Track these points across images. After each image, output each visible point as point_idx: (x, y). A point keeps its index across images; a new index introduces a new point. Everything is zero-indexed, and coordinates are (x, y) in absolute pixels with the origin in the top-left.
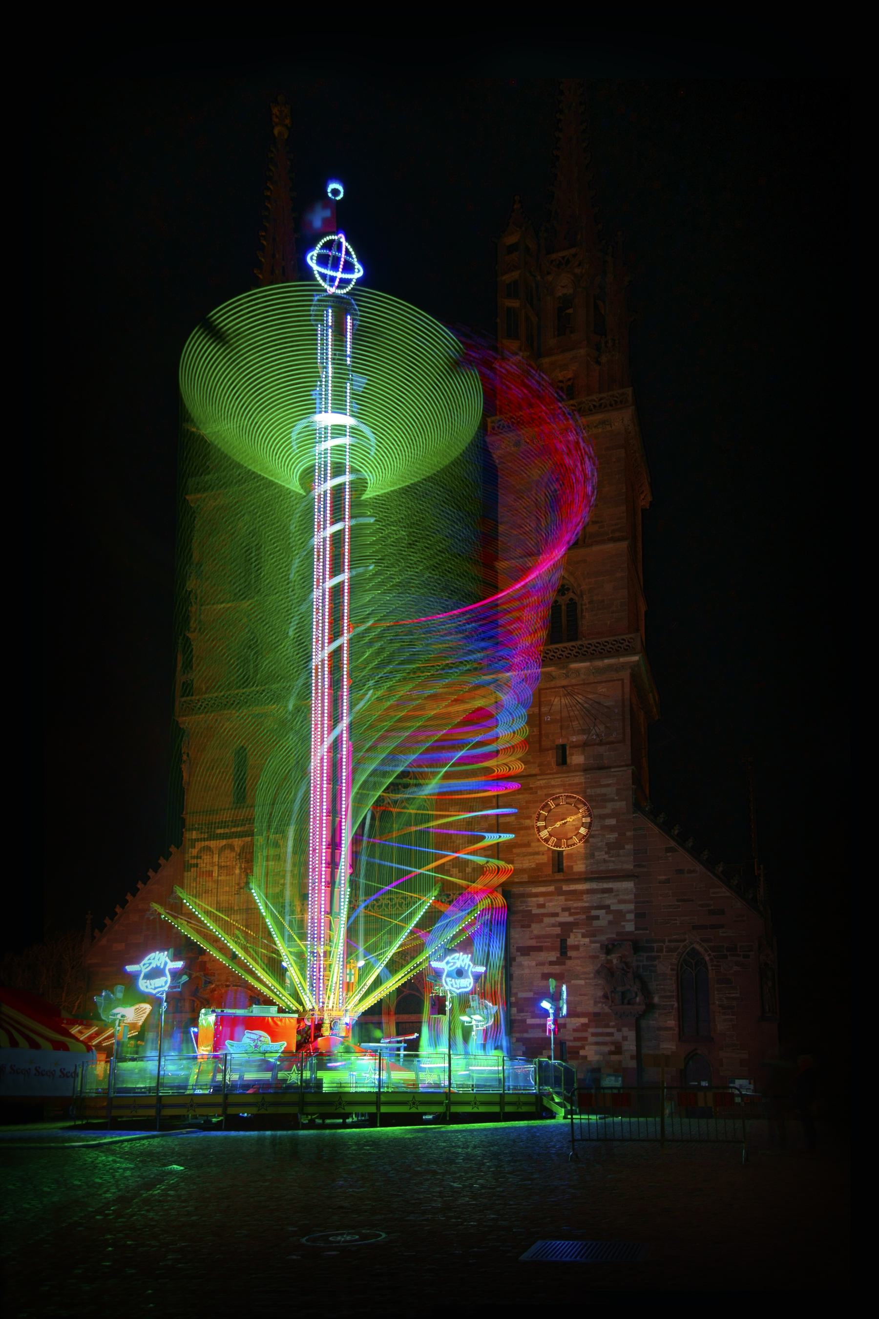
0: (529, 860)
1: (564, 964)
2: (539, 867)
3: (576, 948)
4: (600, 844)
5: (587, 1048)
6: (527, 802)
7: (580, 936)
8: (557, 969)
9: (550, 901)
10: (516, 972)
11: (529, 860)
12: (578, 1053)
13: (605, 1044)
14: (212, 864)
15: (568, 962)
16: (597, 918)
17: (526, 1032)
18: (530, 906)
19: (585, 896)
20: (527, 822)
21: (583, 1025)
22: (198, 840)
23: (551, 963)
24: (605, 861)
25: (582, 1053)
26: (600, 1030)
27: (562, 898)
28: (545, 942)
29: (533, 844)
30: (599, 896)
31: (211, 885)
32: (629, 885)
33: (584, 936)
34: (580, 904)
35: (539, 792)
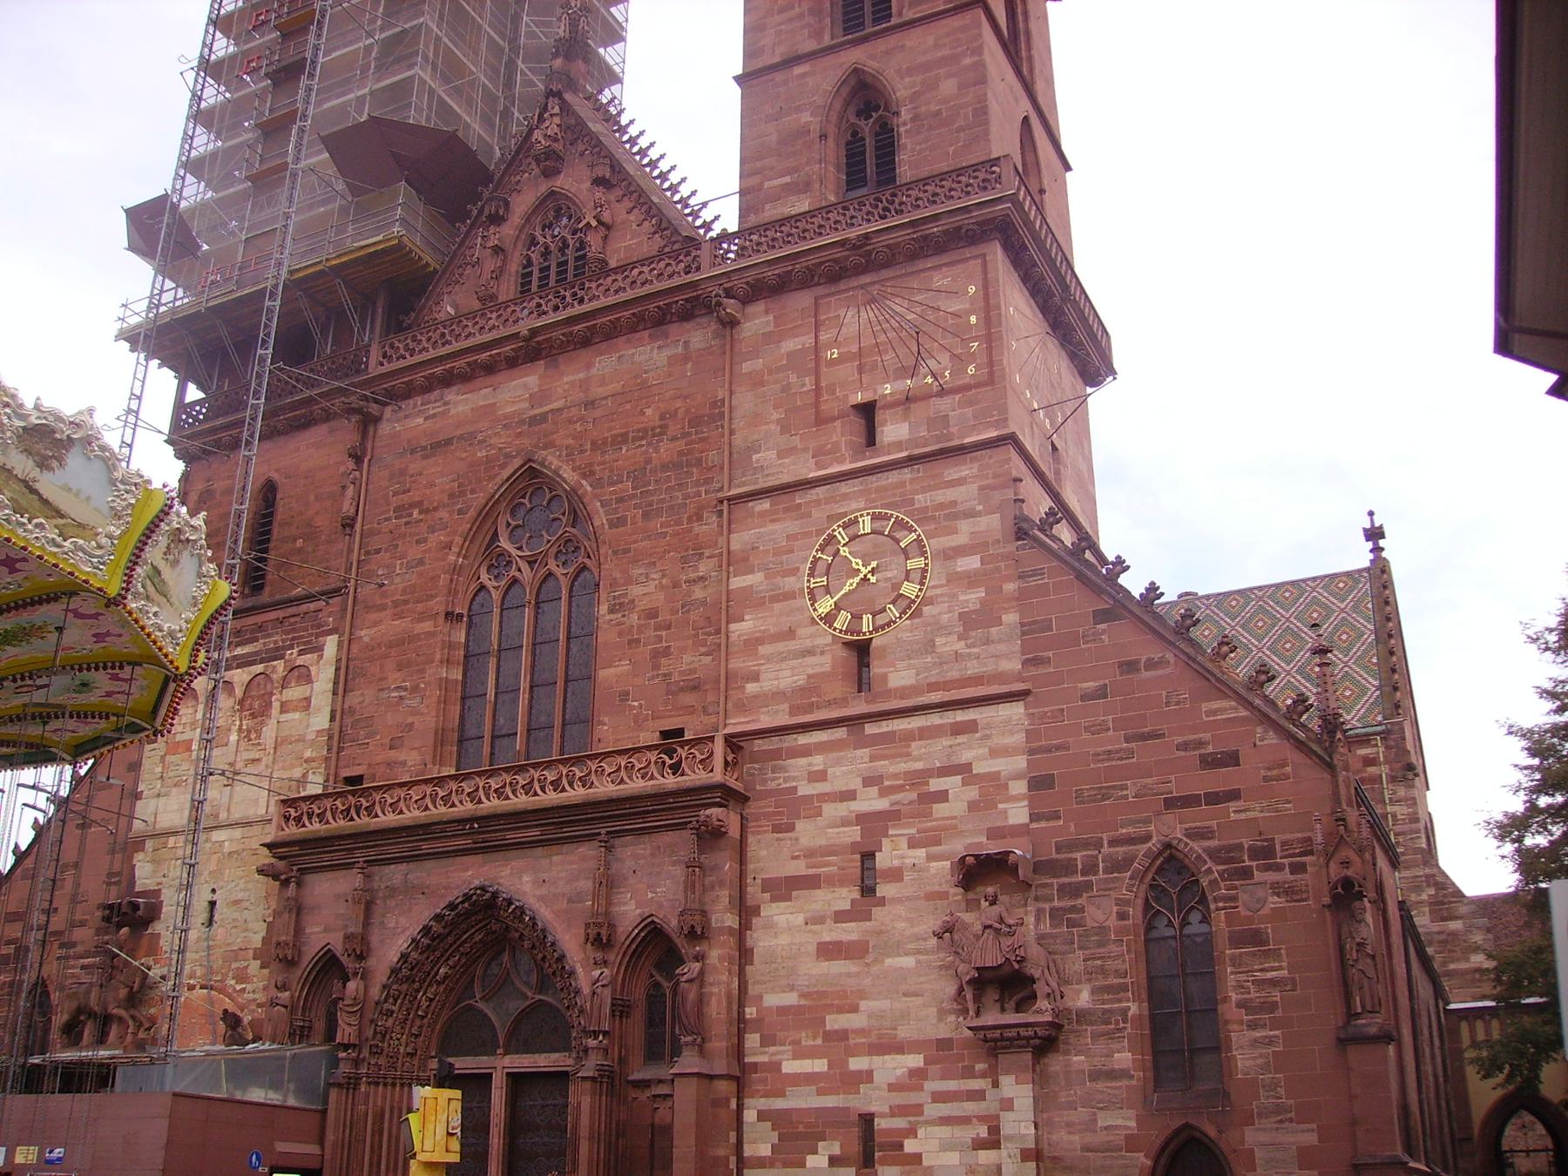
0: (793, 668)
3: (895, 875)
5: (921, 1132)
7: (904, 843)
8: (850, 932)
9: (837, 763)
10: (761, 941)
12: (901, 1146)
13: (964, 1120)
15: (877, 912)
16: (942, 796)
18: (794, 779)
19: (914, 744)
20: (789, 583)
23: (840, 917)
24: (957, 656)
25: (910, 1146)
26: (952, 1085)
29: (801, 632)
30: (946, 742)
32: (1016, 710)
33: (913, 844)
34: (903, 766)
35: (816, 514)
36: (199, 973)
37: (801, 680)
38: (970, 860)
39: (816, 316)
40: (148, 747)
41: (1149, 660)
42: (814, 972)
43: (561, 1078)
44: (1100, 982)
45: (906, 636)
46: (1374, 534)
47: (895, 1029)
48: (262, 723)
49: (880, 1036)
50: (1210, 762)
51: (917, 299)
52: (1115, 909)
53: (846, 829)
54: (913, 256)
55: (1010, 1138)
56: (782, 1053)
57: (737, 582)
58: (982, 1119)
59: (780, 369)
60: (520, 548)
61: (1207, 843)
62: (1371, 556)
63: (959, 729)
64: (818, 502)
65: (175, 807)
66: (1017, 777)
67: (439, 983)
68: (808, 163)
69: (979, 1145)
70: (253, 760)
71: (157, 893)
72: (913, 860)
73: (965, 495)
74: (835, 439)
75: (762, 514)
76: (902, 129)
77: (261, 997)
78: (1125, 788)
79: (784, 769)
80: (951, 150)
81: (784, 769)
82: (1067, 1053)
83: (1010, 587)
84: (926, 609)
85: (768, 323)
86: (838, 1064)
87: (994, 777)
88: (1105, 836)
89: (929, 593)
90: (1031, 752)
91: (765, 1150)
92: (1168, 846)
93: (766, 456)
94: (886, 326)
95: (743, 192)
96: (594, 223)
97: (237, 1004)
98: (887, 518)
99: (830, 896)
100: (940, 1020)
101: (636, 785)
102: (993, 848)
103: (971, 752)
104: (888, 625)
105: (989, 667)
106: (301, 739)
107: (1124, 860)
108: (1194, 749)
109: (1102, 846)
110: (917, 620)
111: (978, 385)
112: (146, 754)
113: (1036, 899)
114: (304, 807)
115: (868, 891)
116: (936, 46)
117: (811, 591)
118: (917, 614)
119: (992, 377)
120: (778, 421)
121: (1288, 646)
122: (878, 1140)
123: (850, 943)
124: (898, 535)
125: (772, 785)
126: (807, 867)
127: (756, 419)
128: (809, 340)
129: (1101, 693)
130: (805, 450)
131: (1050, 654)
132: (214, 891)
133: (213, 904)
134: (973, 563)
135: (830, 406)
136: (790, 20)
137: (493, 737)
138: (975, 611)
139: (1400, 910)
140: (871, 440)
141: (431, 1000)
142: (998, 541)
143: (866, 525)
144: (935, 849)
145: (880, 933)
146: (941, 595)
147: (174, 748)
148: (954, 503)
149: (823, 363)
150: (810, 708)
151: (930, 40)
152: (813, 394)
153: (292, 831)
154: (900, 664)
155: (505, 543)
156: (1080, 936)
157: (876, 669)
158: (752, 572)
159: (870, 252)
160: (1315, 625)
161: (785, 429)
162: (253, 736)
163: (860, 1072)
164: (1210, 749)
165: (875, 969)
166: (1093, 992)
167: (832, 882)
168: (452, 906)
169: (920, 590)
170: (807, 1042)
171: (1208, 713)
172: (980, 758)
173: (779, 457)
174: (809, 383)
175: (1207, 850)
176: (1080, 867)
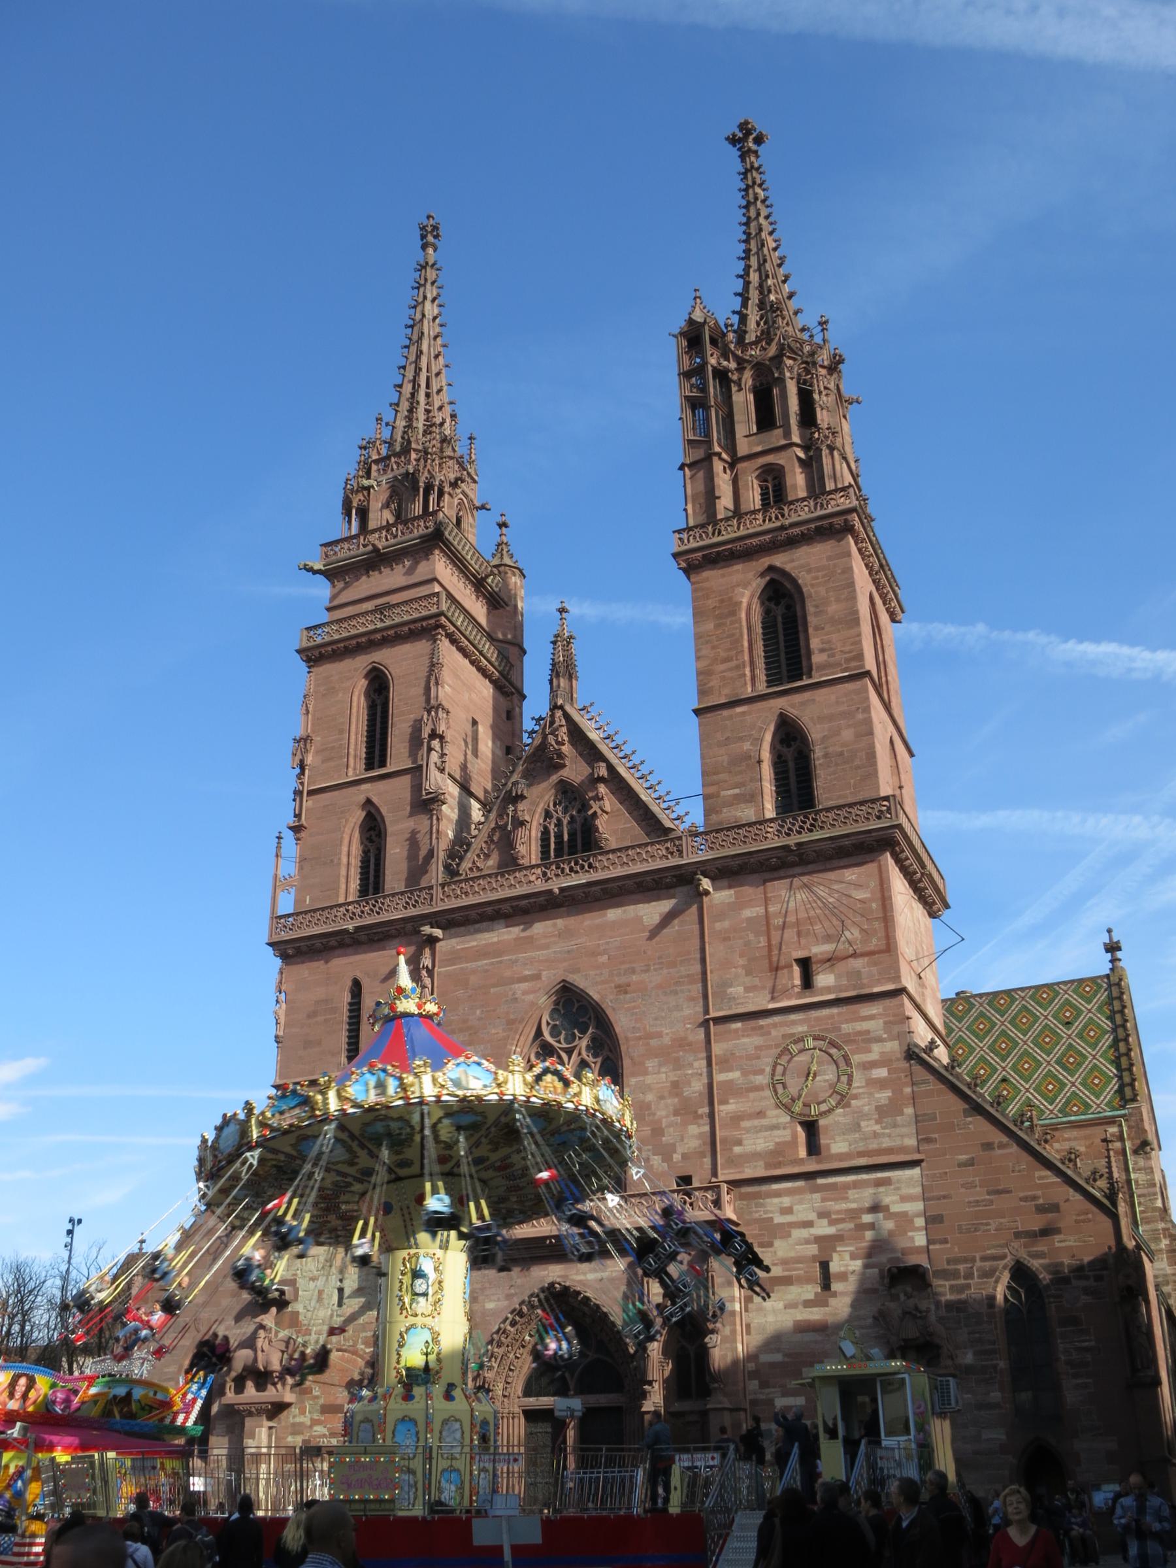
0: (765, 1138)
4: (866, 1108)
6: (757, 1048)
7: (847, 1256)
9: (801, 1202)
11: (765, 1138)
15: (833, 1301)
18: (772, 1212)
19: (850, 1192)
23: (808, 1304)
24: (876, 1135)
27: (817, 1196)
28: (795, 1270)
30: (871, 1191)
32: (916, 1171)
35: (774, 1033)
38: (895, 1270)
41: (1000, 1142)
43: (618, 1410)
45: (841, 1119)
46: (1112, 948)
50: (1041, 1209)
51: (835, 887)
53: (808, 1246)
54: (830, 858)
60: (559, 1042)
61: (1042, 1261)
62: (1110, 966)
63: (879, 1183)
64: (775, 1025)
66: (918, 1215)
68: (752, 780)
72: (854, 1268)
73: (875, 1026)
75: (736, 1030)
76: (817, 763)
78: (988, 1224)
79: (763, 1205)
80: (852, 781)
83: (908, 1090)
84: (853, 1102)
85: (731, 896)
87: (904, 1214)
89: (854, 1091)
93: (737, 990)
94: (814, 905)
95: (706, 797)
96: (599, 812)
99: (800, 1290)
105: (897, 1142)
108: (1032, 1201)
109: (975, 1261)
110: (847, 1109)
111: (879, 952)
115: (826, 1284)
116: (837, 703)
118: (848, 1105)
119: (889, 947)
120: (743, 967)
121: (1047, 1040)
125: (757, 1215)
128: (761, 910)
129: (971, 1163)
130: (763, 988)
131: (936, 1136)
134: (882, 1073)
136: (731, 669)
138: (885, 1105)
139: (1157, 1290)
140: (807, 983)
142: (898, 1060)
146: (863, 1093)
148: (868, 1032)
149: (772, 927)
150: (779, 1165)
151: (833, 697)
152: (766, 950)
154: (838, 1138)
155: (548, 1037)
157: (823, 1141)
158: (730, 1070)
159: (803, 854)
160: (1068, 1023)
164: (1041, 1201)
166: (975, 1354)
167: (800, 1281)
169: (849, 1089)
171: (1041, 1178)
172: (894, 1203)
173: (748, 992)
174: (763, 941)
175: (1041, 1265)
176: (962, 1274)
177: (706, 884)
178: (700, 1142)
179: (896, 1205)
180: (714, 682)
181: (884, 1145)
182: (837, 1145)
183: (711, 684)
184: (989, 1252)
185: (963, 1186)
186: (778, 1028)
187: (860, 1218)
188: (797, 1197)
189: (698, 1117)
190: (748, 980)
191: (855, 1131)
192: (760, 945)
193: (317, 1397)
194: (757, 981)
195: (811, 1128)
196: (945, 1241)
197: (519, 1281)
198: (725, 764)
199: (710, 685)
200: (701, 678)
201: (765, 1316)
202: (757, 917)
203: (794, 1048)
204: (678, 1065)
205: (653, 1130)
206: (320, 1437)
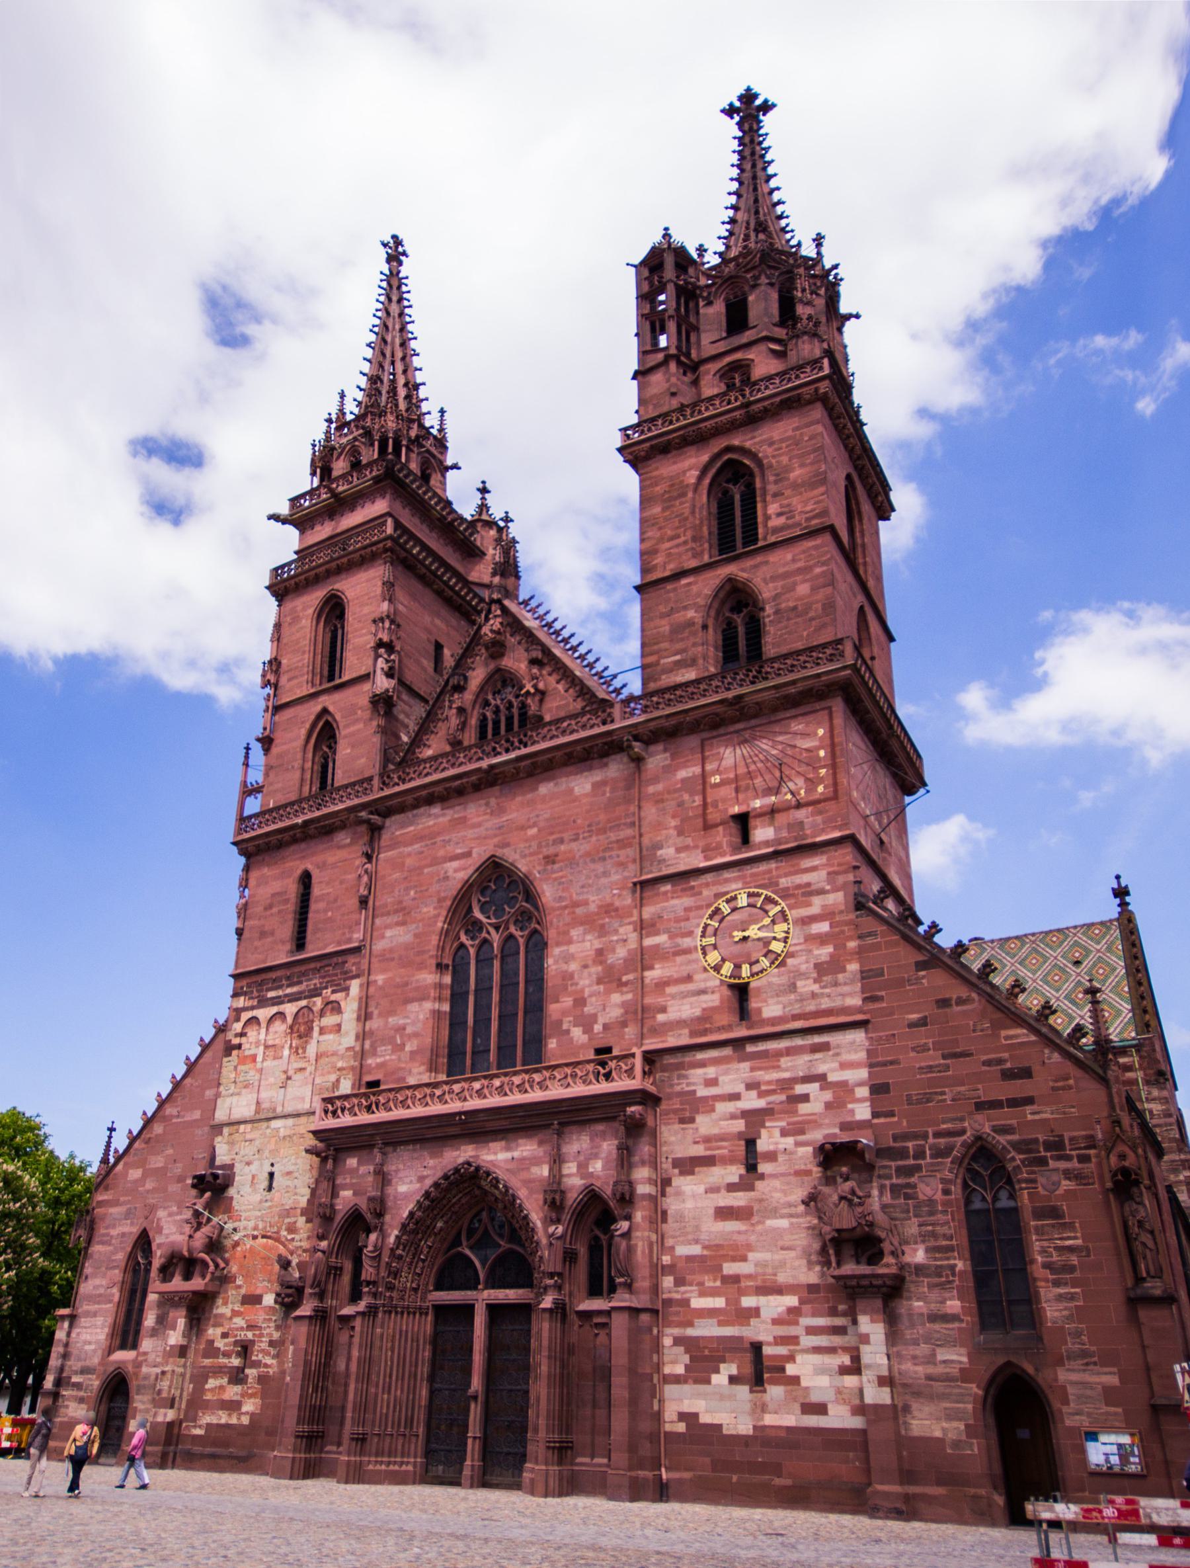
1: (751, 1188)
2: (706, 1016)
3: (772, 1156)
4: (803, 967)
5: (799, 1358)
6: (687, 910)
7: (777, 1133)
8: (739, 1199)
9: (726, 1073)
10: (672, 1204)
12: (783, 1369)
13: (831, 1350)
14: (257, 1044)
15: (759, 1184)
16: (805, 1098)
17: (690, 1324)
18: (694, 1084)
20: (686, 942)
21: (790, 1310)
22: (245, 1009)
23: (731, 1187)
24: (814, 995)
25: (790, 1370)
27: (746, 1065)
29: (697, 977)
30: (807, 1057)
31: (252, 1076)
32: (858, 1036)
33: (784, 1133)
36: (261, 1226)
37: (697, 1012)
38: (828, 1146)
39: (703, 752)
40: (225, 1059)
42: (713, 1229)
44: (932, 1243)
45: (775, 980)
47: (775, 1275)
48: (306, 1042)
49: (764, 1281)
52: (940, 1186)
55: (869, 1366)
56: (691, 1291)
57: (648, 942)
58: (845, 1349)
59: (676, 791)
63: (815, 1049)
64: (707, 885)
65: (244, 1103)
66: (860, 1084)
67: (436, 1235)
69: (844, 1371)
70: (302, 1069)
71: (231, 1166)
74: (718, 839)
75: (666, 893)
77: (305, 1244)
79: (686, 1077)
81: (686, 1077)
82: (909, 1299)
84: (790, 961)
86: (733, 1302)
87: (843, 1085)
88: (930, 1130)
90: (871, 1066)
91: (680, 1370)
92: (978, 1138)
93: (667, 852)
95: (644, 667)
97: (288, 1250)
98: (758, 895)
100: (809, 1269)
101: (578, 1090)
102: (845, 1138)
103: (825, 1065)
104: (761, 972)
105: (838, 1003)
106: (334, 1054)
107: (946, 1148)
110: (783, 969)
112: (224, 1064)
113: (880, 1177)
114: (338, 1103)
115: (751, 1168)
117: (703, 948)
120: (676, 827)
122: (766, 1363)
123: (739, 1207)
124: (767, 907)
125: (678, 1088)
126: (707, 1149)
127: (659, 826)
128: (697, 770)
130: (696, 847)
132: (272, 1165)
133: (271, 1175)
135: (713, 816)
136: (678, 546)
137: (474, 1053)
141: (430, 1247)
143: (743, 901)
144: (801, 1138)
145: (761, 1201)
147: (243, 1060)
150: (705, 1032)
152: (701, 809)
153: (331, 1123)
154: (771, 1001)
156: (914, 1207)
157: (753, 1004)
158: (657, 933)
161: (680, 833)
162: (300, 1051)
163: (749, 1309)
165: (759, 1228)
166: (927, 1250)
168: (446, 1177)
170: (709, 1284)
174: (698, 800)
176: (912, 1153)
177: (637, 747)
178: (622, 1011)
179: (836, 1073)
180: (659, 560)
181: (823, 1006)
182: (770, 1008)
183: (655, 562)
184: (945, 1126)
185: (913, 1049)
186: (708, 888)
187: (793, 1088)
188: (724, 1067)
189: (621, 984)
190: (680, 841)
191: (791, 992)
192: (695, 804)
193: (239, 1287)
194: (689, 841)
195: (741, 992)
196: (891, 1114)
197: (432, 1162)
198: (667, 633)
199: (655, 562)
200: (645, 557)
201: (684, 1201)
202: (694, 776)
203: (726, 909)
204: (602, 931)
205: (575, 1000)
206: (237, 1329)
